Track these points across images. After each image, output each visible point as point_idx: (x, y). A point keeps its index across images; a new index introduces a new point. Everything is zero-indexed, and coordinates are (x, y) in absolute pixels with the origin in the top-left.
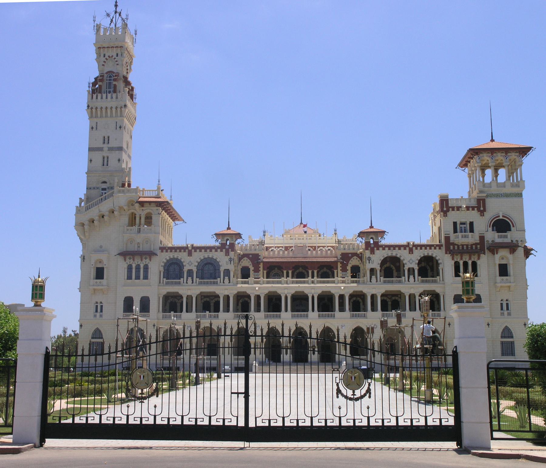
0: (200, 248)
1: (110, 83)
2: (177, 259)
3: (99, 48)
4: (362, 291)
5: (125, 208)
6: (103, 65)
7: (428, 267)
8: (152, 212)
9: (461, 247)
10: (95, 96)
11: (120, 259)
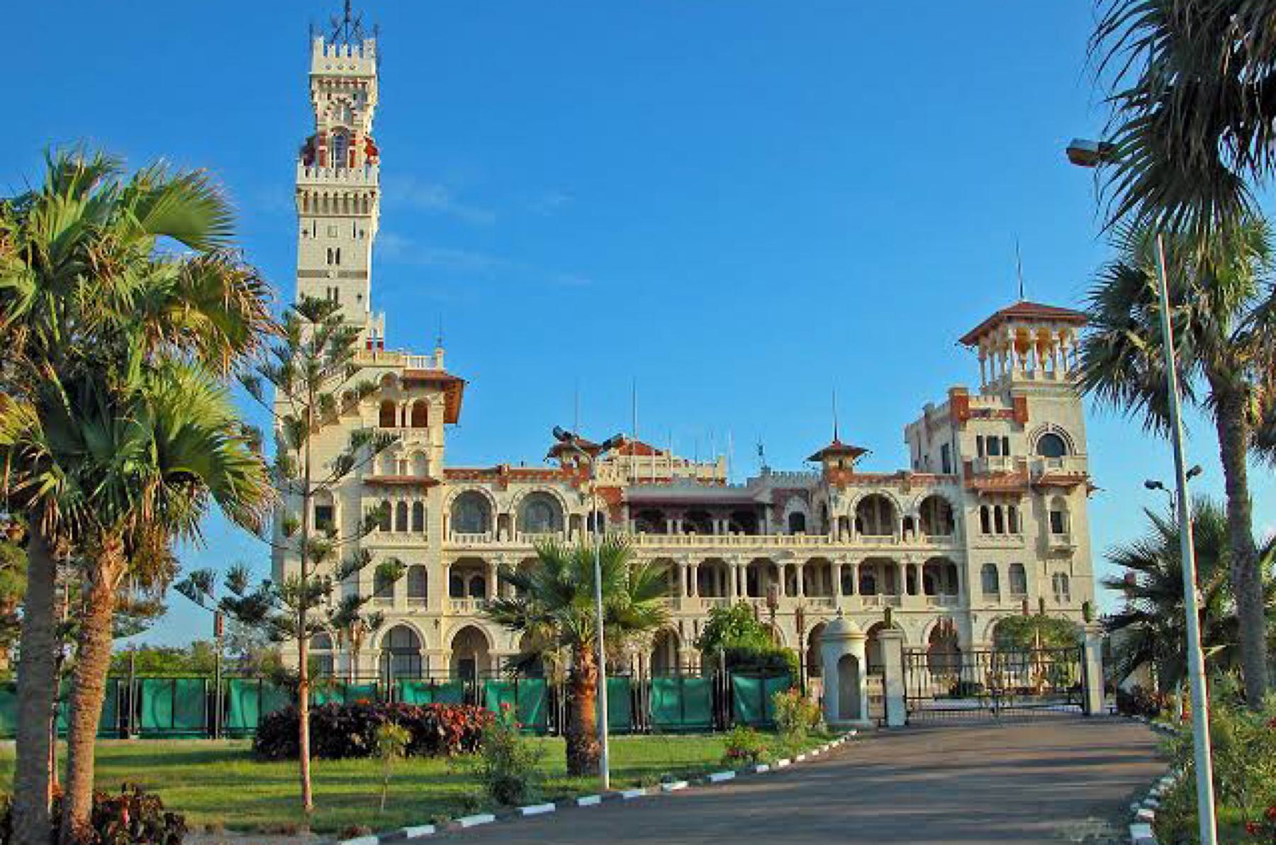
0: (523, 475)
7: (938, 515)
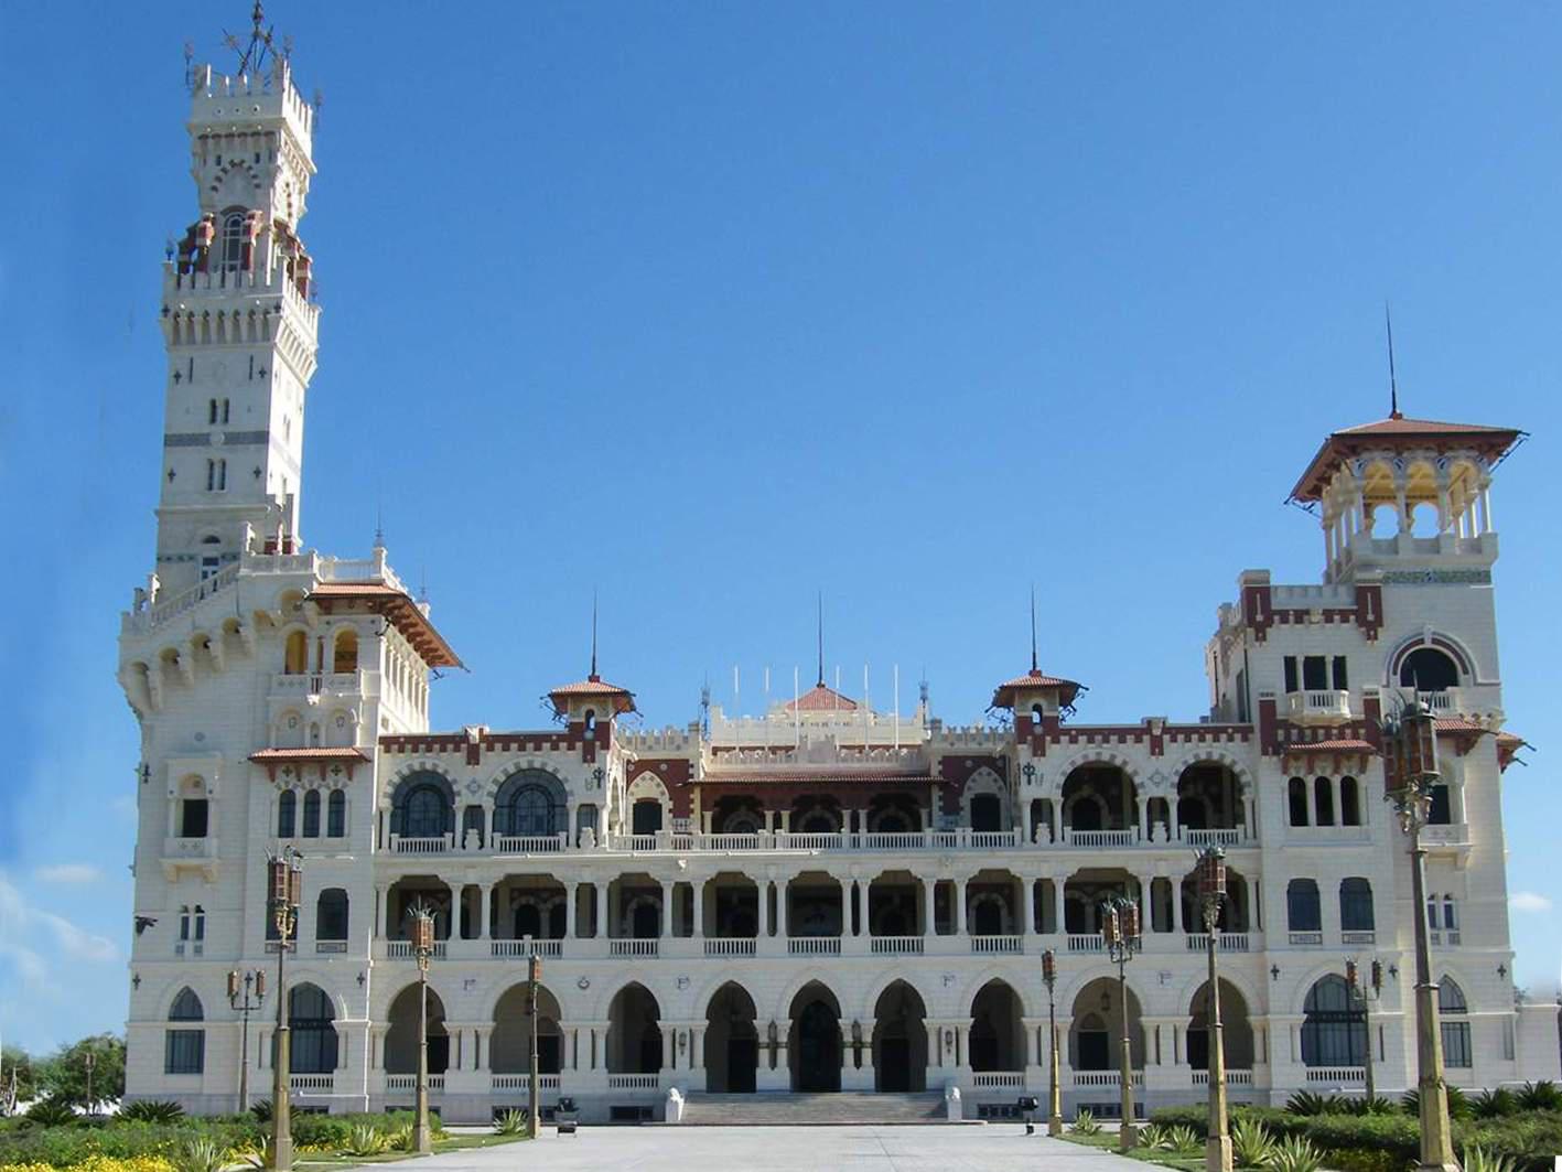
0: (506, 741)
1: (234, 243)
2: (434, 773)
3: (204, 137)
4: (1006, 871)
5: (277, 614)
6: (214, 189)
7: (1209, 797)
8: (357, 629)
9: (1308, 732)
10: (186, 279)
11: (259, 773)
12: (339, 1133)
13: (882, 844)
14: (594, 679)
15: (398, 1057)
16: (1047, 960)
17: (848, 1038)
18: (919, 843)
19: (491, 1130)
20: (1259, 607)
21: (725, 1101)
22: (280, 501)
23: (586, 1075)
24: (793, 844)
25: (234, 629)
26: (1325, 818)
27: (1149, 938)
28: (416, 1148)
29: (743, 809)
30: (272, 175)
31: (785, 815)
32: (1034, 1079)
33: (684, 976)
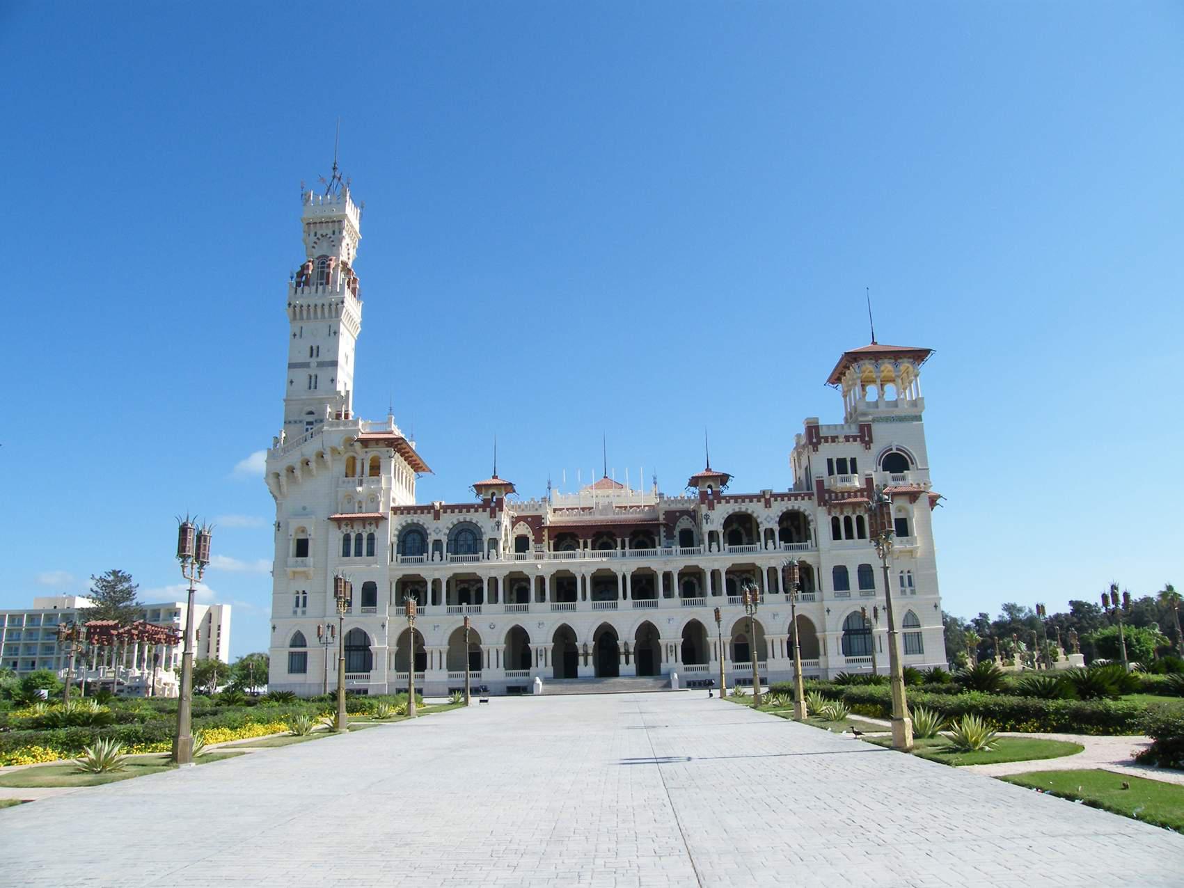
0: (453, 508)
1: (322, 272)
3: (309, 224)
7: (794, 528)
11: (333, 525)
12: (371, 707)
13: (638, 554)
14: (495, 477)
15: (401, 665)
16: (717, 612)
17: (622, 650)
18: (655, 554)
19: (446, 701)
20: (814, 435)
21: (562, 683)
22: (343, 394)
23: (494, 672)
24: (593, 556)
25: (321, 456)
26: (849, 536)
27: (768, 596)
28: (409, 714)
29: (569, 539)
30: (341, 240)
31: (589, 541)
32: (713, 667)
33: (541, 620)
